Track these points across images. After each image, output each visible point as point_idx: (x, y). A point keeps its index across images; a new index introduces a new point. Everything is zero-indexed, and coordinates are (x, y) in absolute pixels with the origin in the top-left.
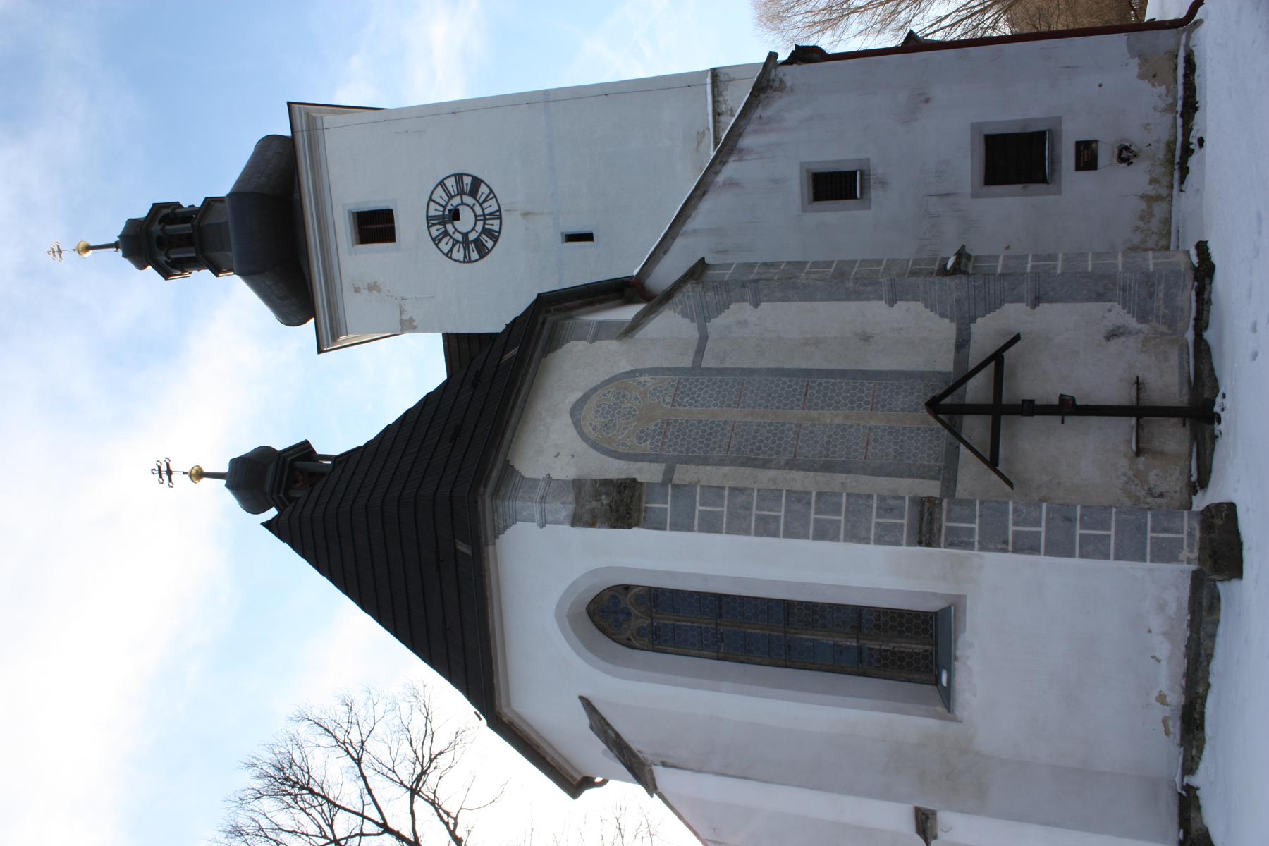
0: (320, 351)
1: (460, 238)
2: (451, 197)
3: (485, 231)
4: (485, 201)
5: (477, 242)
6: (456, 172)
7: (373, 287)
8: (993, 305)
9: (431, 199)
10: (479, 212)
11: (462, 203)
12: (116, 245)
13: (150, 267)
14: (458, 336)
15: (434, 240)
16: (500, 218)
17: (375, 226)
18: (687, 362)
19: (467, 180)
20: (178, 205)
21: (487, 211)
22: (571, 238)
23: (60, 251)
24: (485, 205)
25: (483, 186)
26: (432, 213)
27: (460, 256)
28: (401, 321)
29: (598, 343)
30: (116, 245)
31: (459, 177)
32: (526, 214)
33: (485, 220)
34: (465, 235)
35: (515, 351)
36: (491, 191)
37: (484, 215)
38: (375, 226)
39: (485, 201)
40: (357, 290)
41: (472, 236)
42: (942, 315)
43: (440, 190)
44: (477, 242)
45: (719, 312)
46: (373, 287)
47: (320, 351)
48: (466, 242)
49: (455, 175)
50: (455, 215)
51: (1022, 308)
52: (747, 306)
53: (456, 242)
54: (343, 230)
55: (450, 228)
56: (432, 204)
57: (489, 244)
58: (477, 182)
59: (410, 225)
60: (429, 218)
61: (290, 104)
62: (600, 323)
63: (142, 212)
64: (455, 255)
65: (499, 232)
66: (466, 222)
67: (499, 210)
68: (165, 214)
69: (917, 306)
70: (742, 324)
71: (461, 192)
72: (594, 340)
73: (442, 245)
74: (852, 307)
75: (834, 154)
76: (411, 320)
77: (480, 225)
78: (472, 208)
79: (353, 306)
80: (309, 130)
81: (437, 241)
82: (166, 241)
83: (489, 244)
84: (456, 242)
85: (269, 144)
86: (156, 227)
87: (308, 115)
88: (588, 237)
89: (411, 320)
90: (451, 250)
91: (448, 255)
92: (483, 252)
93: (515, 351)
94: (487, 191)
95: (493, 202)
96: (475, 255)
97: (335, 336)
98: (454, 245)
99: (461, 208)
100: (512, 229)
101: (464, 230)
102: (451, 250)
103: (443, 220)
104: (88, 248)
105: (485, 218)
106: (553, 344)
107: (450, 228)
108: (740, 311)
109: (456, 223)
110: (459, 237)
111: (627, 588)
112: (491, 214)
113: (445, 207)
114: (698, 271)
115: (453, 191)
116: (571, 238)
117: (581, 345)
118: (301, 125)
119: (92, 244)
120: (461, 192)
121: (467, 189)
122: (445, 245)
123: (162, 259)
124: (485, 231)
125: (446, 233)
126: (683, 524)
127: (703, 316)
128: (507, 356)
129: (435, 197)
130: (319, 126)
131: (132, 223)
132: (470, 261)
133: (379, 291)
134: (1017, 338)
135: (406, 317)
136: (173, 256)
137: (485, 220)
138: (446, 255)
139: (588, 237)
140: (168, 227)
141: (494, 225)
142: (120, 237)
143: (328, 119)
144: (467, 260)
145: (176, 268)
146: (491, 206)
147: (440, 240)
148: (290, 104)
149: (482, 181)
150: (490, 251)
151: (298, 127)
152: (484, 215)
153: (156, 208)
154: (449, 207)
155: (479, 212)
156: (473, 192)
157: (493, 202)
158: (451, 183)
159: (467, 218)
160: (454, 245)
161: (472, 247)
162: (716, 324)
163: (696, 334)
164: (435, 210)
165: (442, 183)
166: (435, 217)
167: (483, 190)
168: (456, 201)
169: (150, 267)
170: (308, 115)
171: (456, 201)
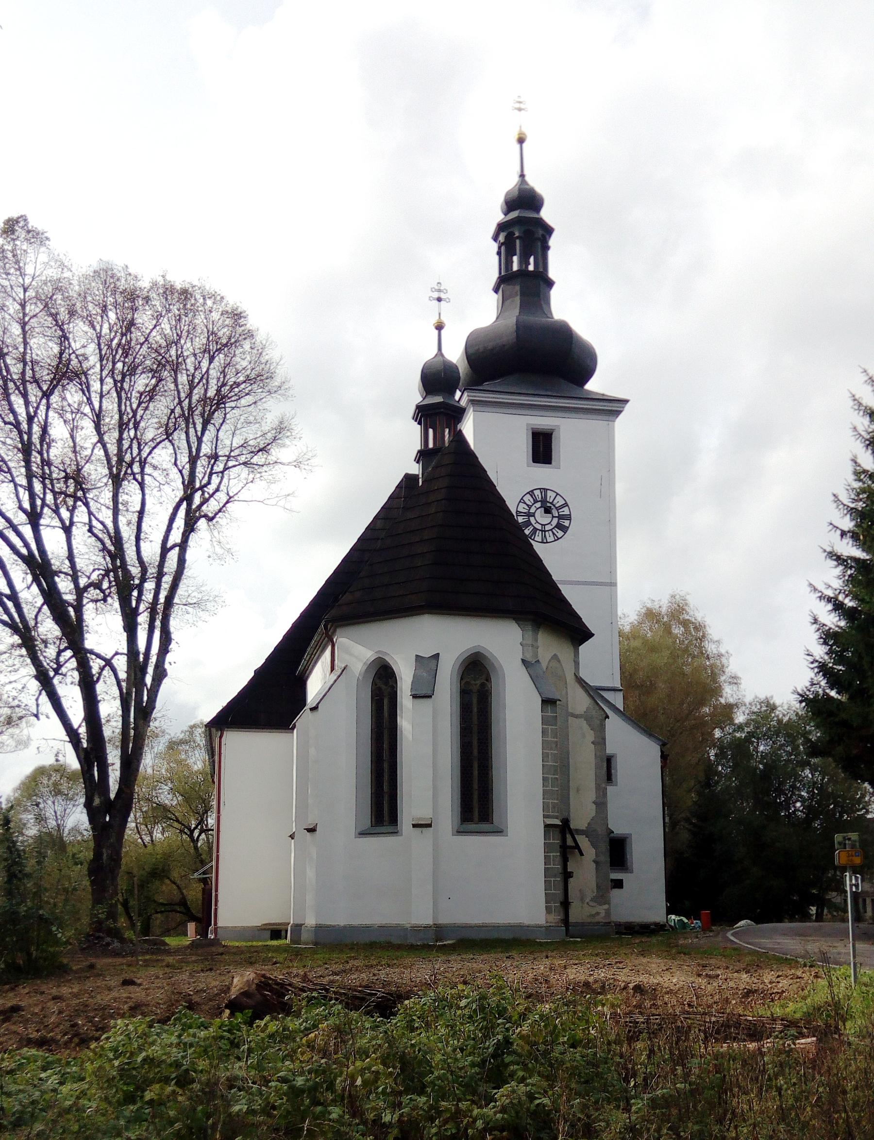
1: (532, 510)
3: (535, 529)
4: (554, 534)
8: (594, 845)
9: (557, 494)
10: (548, 528)
11: (553, 517)
12: (522, 176)
15: (532, 491)
18: (570, 710)
19: (566, 523)
26: (549, 493)
30: (522, 176)
31: (568, 517)
33: (542, 531)
34: (533, 515)
36: (558, 539)
37: (545, 531)
39: (554, 534)
41: (532, 519)
42: (589, 824)
45: (590, 725)
51: (594, 857)
52: (593, 739)
53: (530, 507)
55: (538, 505)
58: (564, 529)
60: (546, 490)
64: (522, 505)
69: (593, 814)
70: (584, 736)
71: (560, 517)
74: (592, 785)
75: (620, 770)
77: (539, 527)
81: (531, 493)
103: (544, 501)
107: (538, 505)
108: (590, 736)
110: (532, 510)
111: (488, 679)
113: (551, 503)
114: (607, 717)
122: (528, 499)
125: (536, 501)
126: (544, 721)
127: (587, 717)
134: (582, 854)
152: (545, 531)
156: (559, 526)
158: (565, 511)
162: (584, 724)
163: (577, 713)
164: (550, 496)
167: (560, 533)
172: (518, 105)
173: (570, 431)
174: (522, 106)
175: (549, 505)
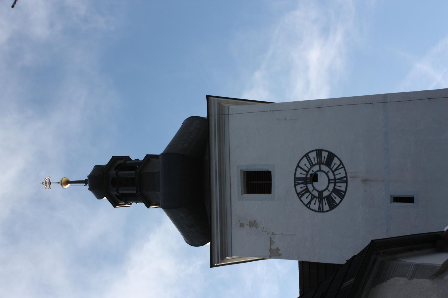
0: (212, 265)
1: (316, 194)
2: (312, 165)
3: (335, 191)
4: (336, 169)
5: (329, 198)
6: (317, 148)
7: (253, 224)
9: (298, 166)
10: (332, 177)
11: (320, 170)
12: (85, 182)
13: (105, 198)
14: (310, 264)
15: (298, 194)
16: (346, 182)
17: (258, 182)
19: (325, 154)
20: (128, 158)
21: (337, 177)
22: (397, 199)
23: (50, 183)
24: (336, 173)
25: (335, 158)
26: (298, 175)
27: (316, 207)
28: (270, 250)
29: (415, 280)
30: (85, 182)
31: (319, 152)
32: (365, 181)
33: (335, 183)
34: (321, 193)
35: (352, 280)
36: (341, 163)
37: (335, 179)
38: (258, 182)
39: (336, 169)
40: (242, 225)
41: (326, 194)
43: (305, 160)
44: (329, 198)
46: (253, 224)
47: (212, 265)
48: (321, 198)
49: (316, 150)
50: (314, 178)
53: (313, 197)
54: (236, 183)
55: (310, 187)
56: (299, 170)
57: (338, 200)
58: (331, 156)
59: (282, 182)
61: (208, 97)
62: (417, 266)
63: (105, 161)
64: (312, 206)
65: (345, 192)
66: (322, 183)
67: (346, 177)
68: (120, 163)
71: (320, 163)
72: (412, 278)
73: (304, 198)
76: (278, 249)
78: (327, 174)
79: (238, 236)
80: (219, 115)
81: (300, 195)
82: (117, 182)
83: (338, 200)
84: (313, 197)
85: (192, 122)
86: (113, 172)
87: (219, 104)
88: (410, 200)
89: (278, 249)
90: (310, 203)
91: (307, 205)
92: (333, 205)
93: (352, 280)
94: (338, 163)
95: (342, 171)
96: (326, 207)
97: (223, 256)
98: (312, 199)
99: (319, 173)
100: (354, 190)
101: (320, 189)
102: (310, 203)
103: (305, 181)
104: (68, 182)
105: (335, 181)
106: (381, 278)
107: (310, 187)
109: (315, 184)
110: (316, 194)
112: (339, 179)
113: (307, 172)
115: (314, 161)
116: (397, 199)
117: (402, 281)
118: (215, 111)
119: (71, 180)
120: (320, 163)
121: (324, 160)
123: (114, 193)
124: (335, 191)
125: (307, 190)
128: (346, 284)
129: (301, 165)
130: (226, 112)
131: (98, 168)
132: (323, 211)
133: (257, 227)
135: (274, 247)
136: (121, 192)
137: (335, 183)
138: (306, 205)
139: (410, 200)
140: (120, 172)
141: (341, 187)
142: (88, 176)
143: (233, 108)
144: (321, 210)
145: (122, 200)
146: (340, 174)
147: (303, 195)
148: (208, 97)
149: (335, 156)
150: (337, 205)
151: (212, 112)
152: (335, 179)
153: (114, 159)
154: (311, 172)
155: (332, 177)
156: (329, 163)
157: (342, 171)
158: (313, 155)
159: (323, 181)
160: (312, 199)
161: (325, 201)
164: (300, 174)
165: (307, 156)
166: (300, 179)
167: (336, 161)
168: (316, 168)
169: (105, 198)
170: (219, 104)
171: (316, 168)
172: (48, 185)
173: (241, 152)
174: (48, 181)
175: (309, 176)
